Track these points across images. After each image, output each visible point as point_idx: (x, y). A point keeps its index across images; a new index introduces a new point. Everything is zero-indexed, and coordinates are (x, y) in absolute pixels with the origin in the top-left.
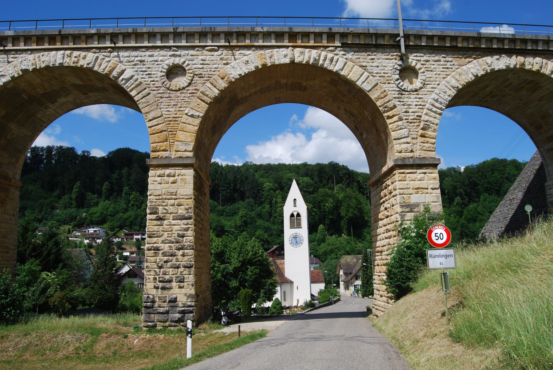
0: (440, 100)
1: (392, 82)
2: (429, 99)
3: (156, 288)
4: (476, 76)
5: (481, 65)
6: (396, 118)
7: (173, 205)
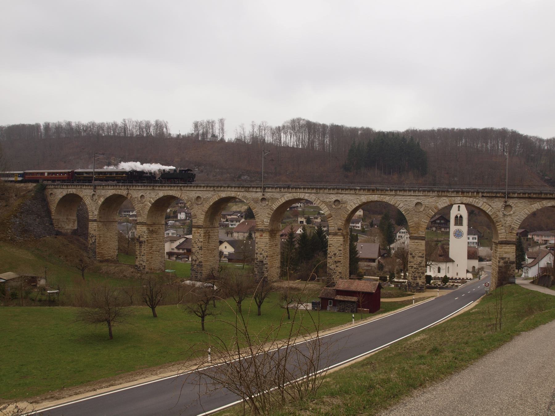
2: (515, 218)
3: (412, 279)
4: (538, 209)
5: (540, 205)
6: (501, 226)
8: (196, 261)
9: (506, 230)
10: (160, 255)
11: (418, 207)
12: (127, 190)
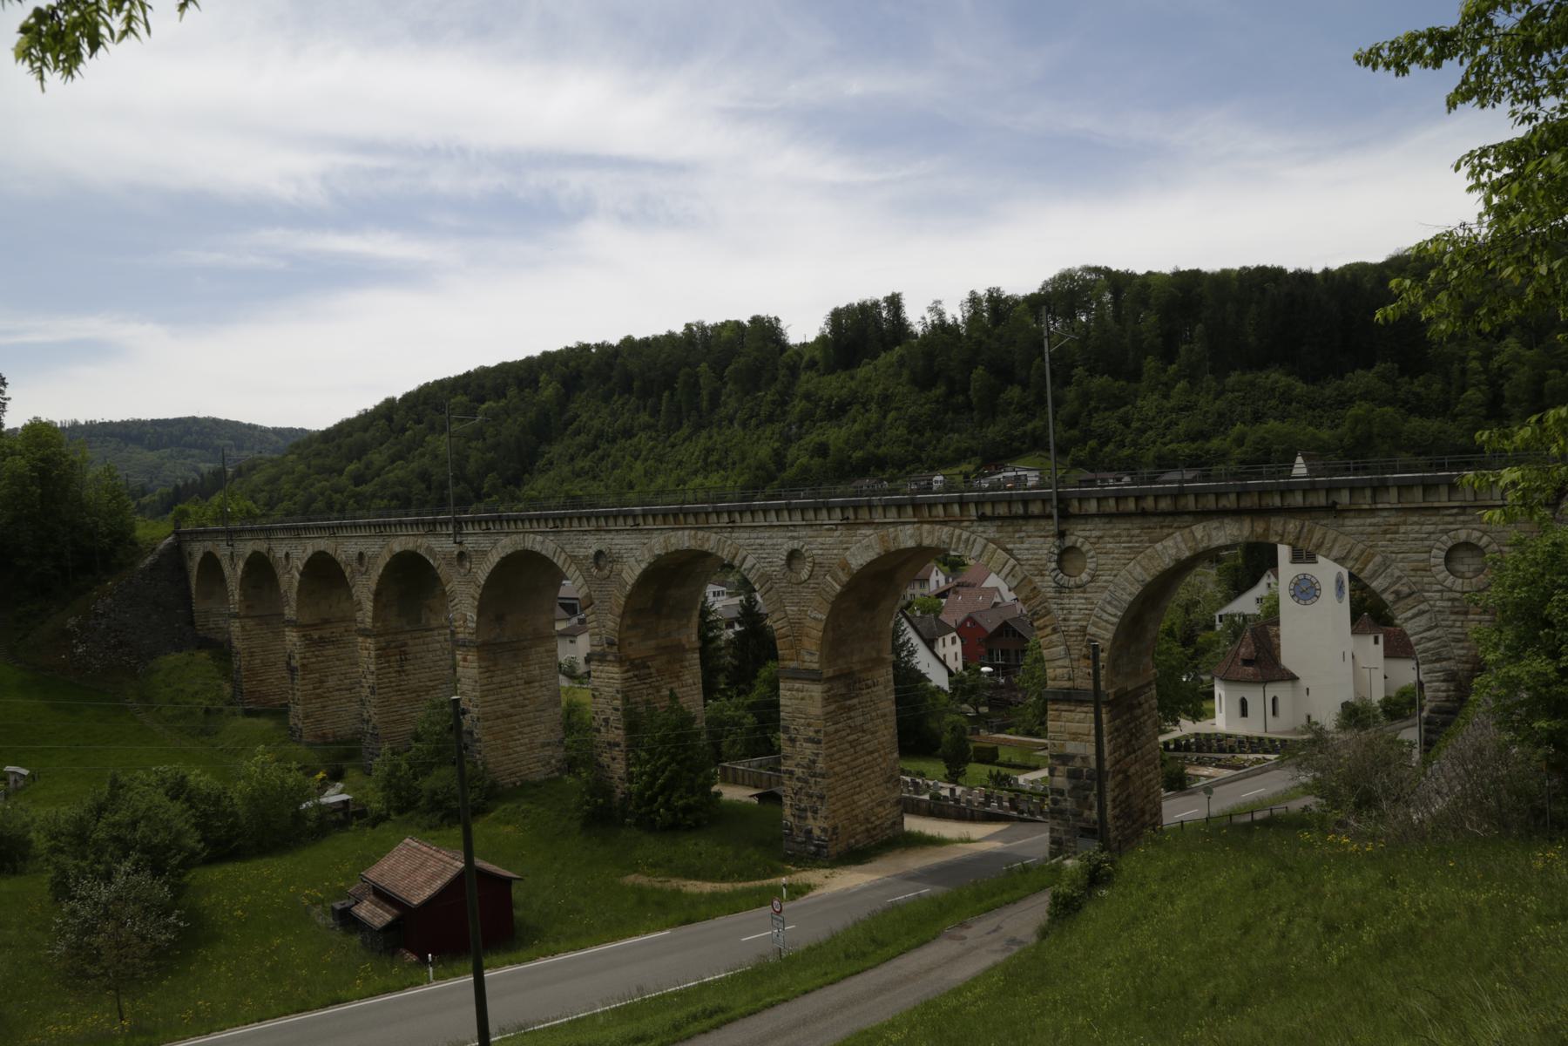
0: (1115, 603)
1: (1047, 573)
3: (794, 816)
5: (1185, 541)
6: (1048, 630)
7: (802, 725)
8: (368, 722)
9: (1068, 648)
10: (354, 699)
11: (796, 564)
12: (267, 541)
